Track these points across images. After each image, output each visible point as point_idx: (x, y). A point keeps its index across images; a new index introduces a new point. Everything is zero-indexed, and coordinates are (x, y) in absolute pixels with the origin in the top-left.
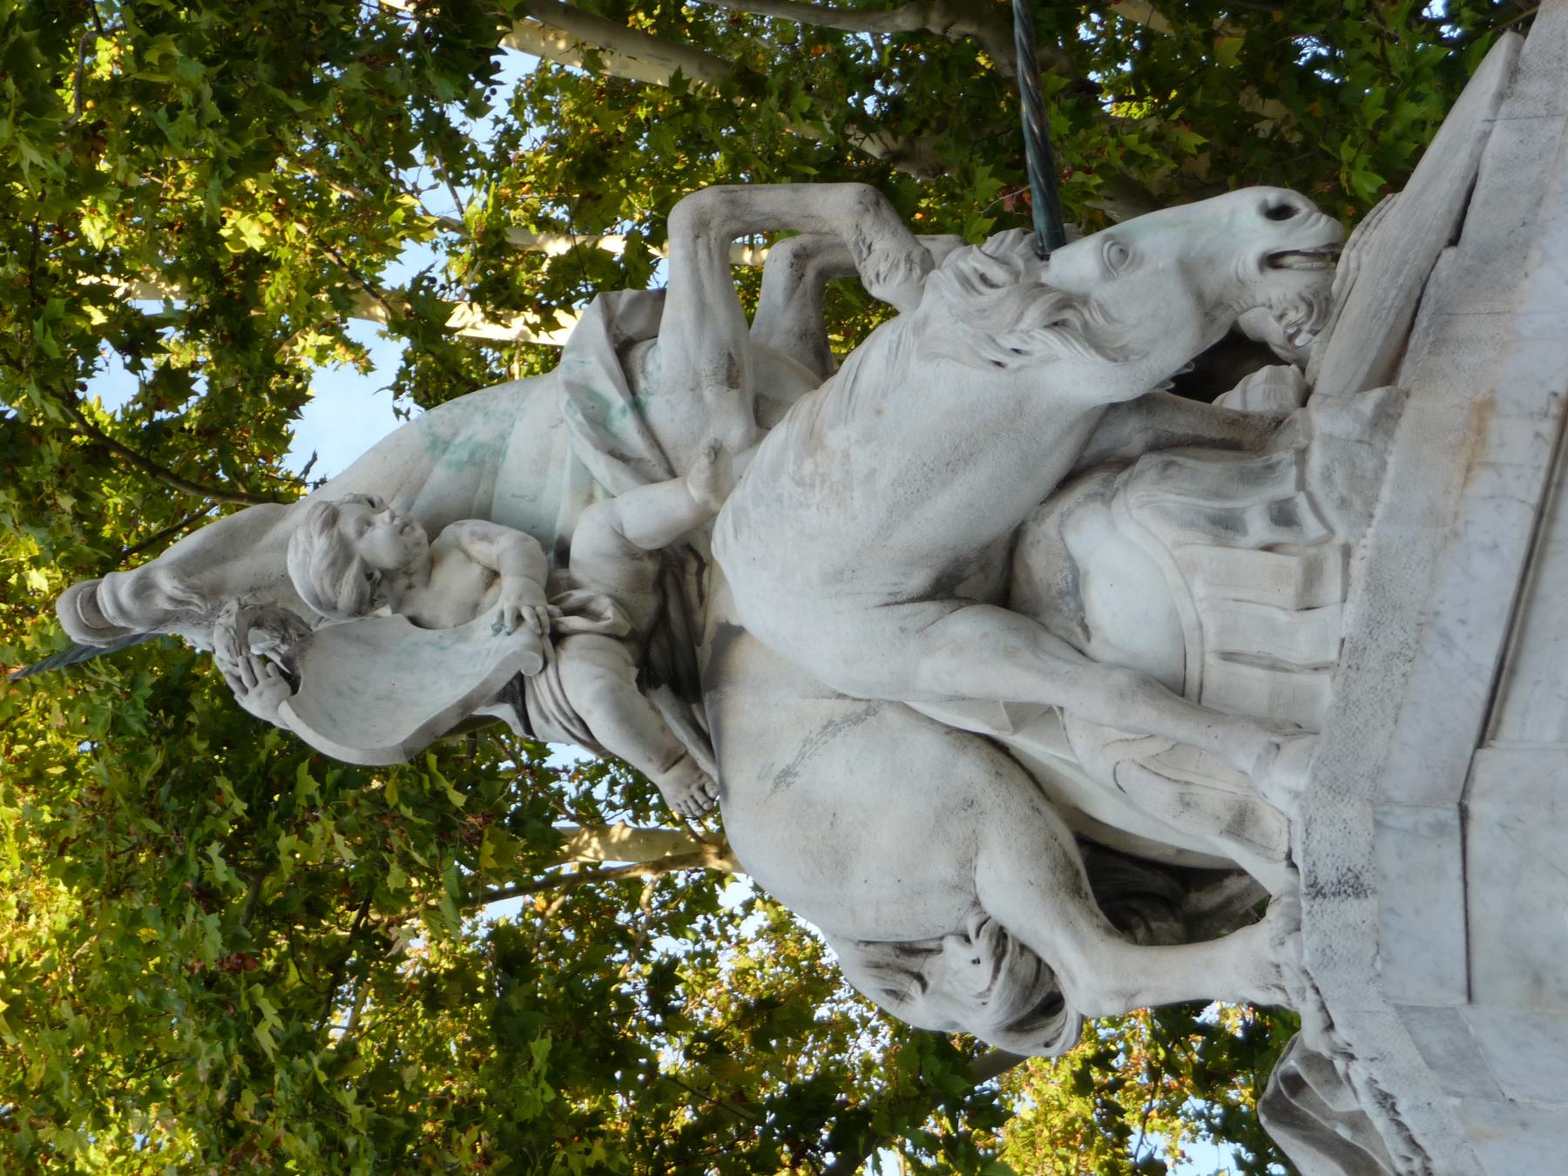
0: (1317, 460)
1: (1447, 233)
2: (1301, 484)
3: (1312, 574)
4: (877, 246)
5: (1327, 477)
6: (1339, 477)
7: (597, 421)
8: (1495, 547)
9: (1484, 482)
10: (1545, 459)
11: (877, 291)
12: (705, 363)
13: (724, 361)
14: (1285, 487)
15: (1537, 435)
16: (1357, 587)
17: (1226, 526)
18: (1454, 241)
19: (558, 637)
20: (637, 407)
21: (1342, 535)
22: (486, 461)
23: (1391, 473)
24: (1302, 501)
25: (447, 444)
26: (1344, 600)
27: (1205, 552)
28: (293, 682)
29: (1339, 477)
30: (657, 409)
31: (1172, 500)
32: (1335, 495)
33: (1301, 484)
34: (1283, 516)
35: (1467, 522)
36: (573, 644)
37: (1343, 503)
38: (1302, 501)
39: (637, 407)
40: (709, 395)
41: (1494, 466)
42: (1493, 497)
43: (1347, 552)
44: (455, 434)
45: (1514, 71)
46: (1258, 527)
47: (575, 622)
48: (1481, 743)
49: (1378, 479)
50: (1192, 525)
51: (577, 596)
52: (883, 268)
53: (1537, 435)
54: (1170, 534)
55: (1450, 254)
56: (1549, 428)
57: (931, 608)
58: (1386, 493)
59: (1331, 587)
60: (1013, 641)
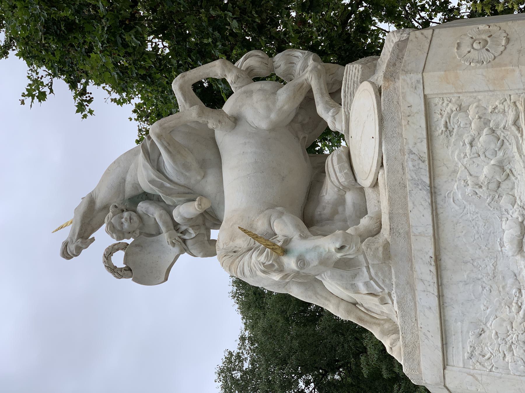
1: (379, 166)
5: (376, 274)
6: (380, 274)
10: (435, 280)
16: (395, 302)
18: (382, 165)
19: (184, 241)
21: (386, 291)
22: (136, 186)
26: (393, 303)
29: (380, 274)
33: (371, 278)
36: (189, 243)
37: (384, 281)
43: (390, 295)
51: (183, 228)
58: (393, 277)
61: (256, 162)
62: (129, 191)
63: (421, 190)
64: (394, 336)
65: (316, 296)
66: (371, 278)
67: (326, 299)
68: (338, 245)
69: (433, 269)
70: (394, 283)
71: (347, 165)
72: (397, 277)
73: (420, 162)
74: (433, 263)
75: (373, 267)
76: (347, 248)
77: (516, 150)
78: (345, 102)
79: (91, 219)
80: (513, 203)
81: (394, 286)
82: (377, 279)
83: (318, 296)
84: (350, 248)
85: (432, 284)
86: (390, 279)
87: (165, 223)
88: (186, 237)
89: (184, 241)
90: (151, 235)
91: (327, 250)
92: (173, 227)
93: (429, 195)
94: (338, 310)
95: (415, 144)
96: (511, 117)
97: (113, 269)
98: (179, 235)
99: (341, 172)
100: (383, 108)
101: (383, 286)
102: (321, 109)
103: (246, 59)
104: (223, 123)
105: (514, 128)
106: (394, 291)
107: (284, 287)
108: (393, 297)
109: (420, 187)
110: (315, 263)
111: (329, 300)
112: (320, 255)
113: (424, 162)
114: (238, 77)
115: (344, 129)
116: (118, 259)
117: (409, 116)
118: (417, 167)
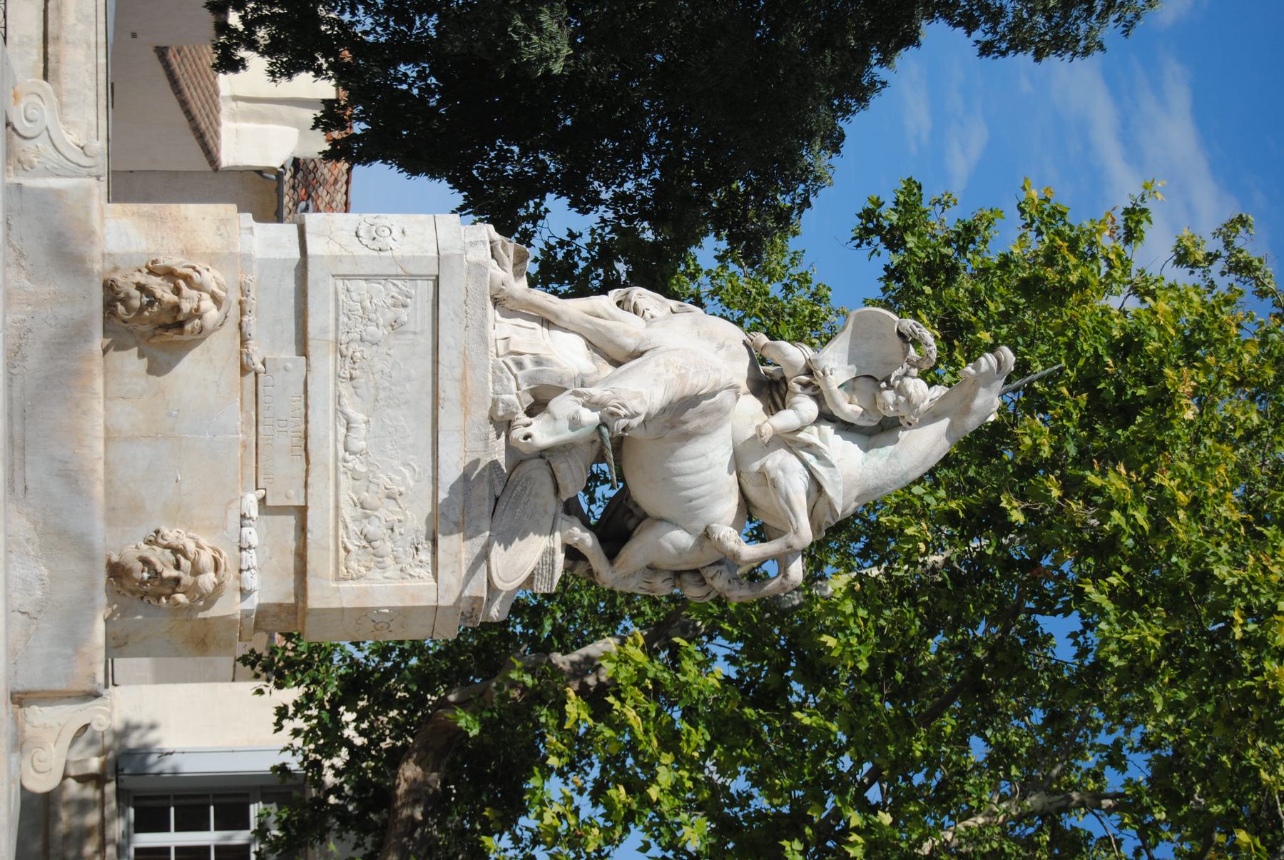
0: (513, 385)
2: (515, 376)
3: (507, 346)
7: (820, 457)
9: (458, 372)
12: (782, 481)
17: (538, 361)
18: (497, 499)
20: (806, 465)
23: (490, 385)
27: (543, 353)
28: (900, 334)
30: (800, 466)
31: (556, 368)
34: (520, 365)
37: (502, 371)
39: (806, 465)
40: (780, 473)
43: (497, 355)
46: (527, 360)
47: (805, 379)
48: (438, 277)
50: (548, 360)
51: (809, 390)
55: (498, 493)
58: (490, 377)
69: (441, 394)
72: (486, 378)
74: (441, 401)
77: (350, 526)
80: (353, 470)
88: (805, 379)
96: (353, 556)
105: (350, 547)
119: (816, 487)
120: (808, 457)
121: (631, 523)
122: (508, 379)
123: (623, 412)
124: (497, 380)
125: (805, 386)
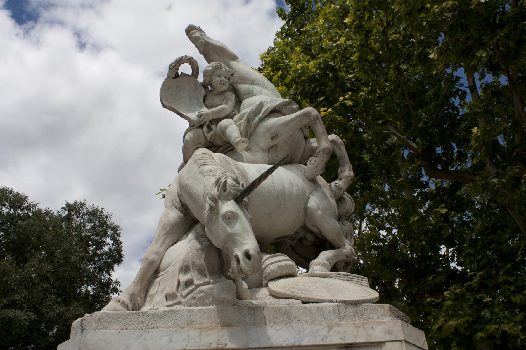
1: (304, 300)
4: (318, 158)
6: (202, 294)
7: (256, 112)
8: (171, 342)
9: (194, 333)
11: (308, 163)
13: (276, 134)
14: (196, 282)
15: (211, 344)
16: (170, 308)
17: (185, 269)
18: (304, 303)
19: (201, 127)
21: (183, 300)
22: (250, 94)
24: (193, 287)
25: (253, 84)
26: (167, 306)
29: (202, 294)
32: (196, 295)
33: (198, 286)
34: (189, 283)
35: (180, 332)
36: (200, 131)
37: (194, 298)
38: (193, 287)
39: (262, 120)
41: (201, 334)
42: (189, 337)
43: (179, 303)
44: (256, 85)
45: (355, 303)
46: (184, 278)
47: (205, 128)
49: (204, 305)
51: (213, 127)
52: (312, 162)
53: (211, 344)
54: (182, 257)
56: (214, 346)
57: (179, 205)
59: (170, 303)
60: (168, 228)
61: (284, 192)
62: (243, 87)
63: (294, 337)
64: (130, 306)
65: (165, 234)
66: (198, 286)
67: (163, 243)
68: (251, 252)
70: (192, 308)
71: (285, 272)
72: (200, 311)
73: (322, 337)
74: (220, 346)
75: (210, 288)
76: (247, 261)
78: (340, 274)
79: (218, 55)
81: (189, 308)
82: (195, 292)
83: (164, 237)
84: (248, 264)
85: (197, 344)
86: (195, 305)
87: (219, 111)
88: (205, 128)
89: (201, 127)
90: (204, 100)
91: (244, 242)
92: (214, 118)
93: (291, 345)
94: (153, 253)
95: (339, 333)
97: (179, 62)
98: (208, 123)
99: (279, 267)
100: (365, 304)
101: (189, 297)
102: (325, 255)
103: (350, 198)
104: (314, 170)
106: (183, 307)
107: (173, 205)
108: (176, 306)
109: (297, 336)
110: (229, 230)
111: (161, 246)
112: (239, 235)
113: (322, 340)
114: (340, 189)
115: (316, 272)
116: (186, 69)
117: (364, 327)
118: (316, 334)
119: (276, 111)
120: (257, 119)
121: (310, 237)
122: (201, 291)
123: (223, 180)
124: (202, 302)
125: (210, 129)
